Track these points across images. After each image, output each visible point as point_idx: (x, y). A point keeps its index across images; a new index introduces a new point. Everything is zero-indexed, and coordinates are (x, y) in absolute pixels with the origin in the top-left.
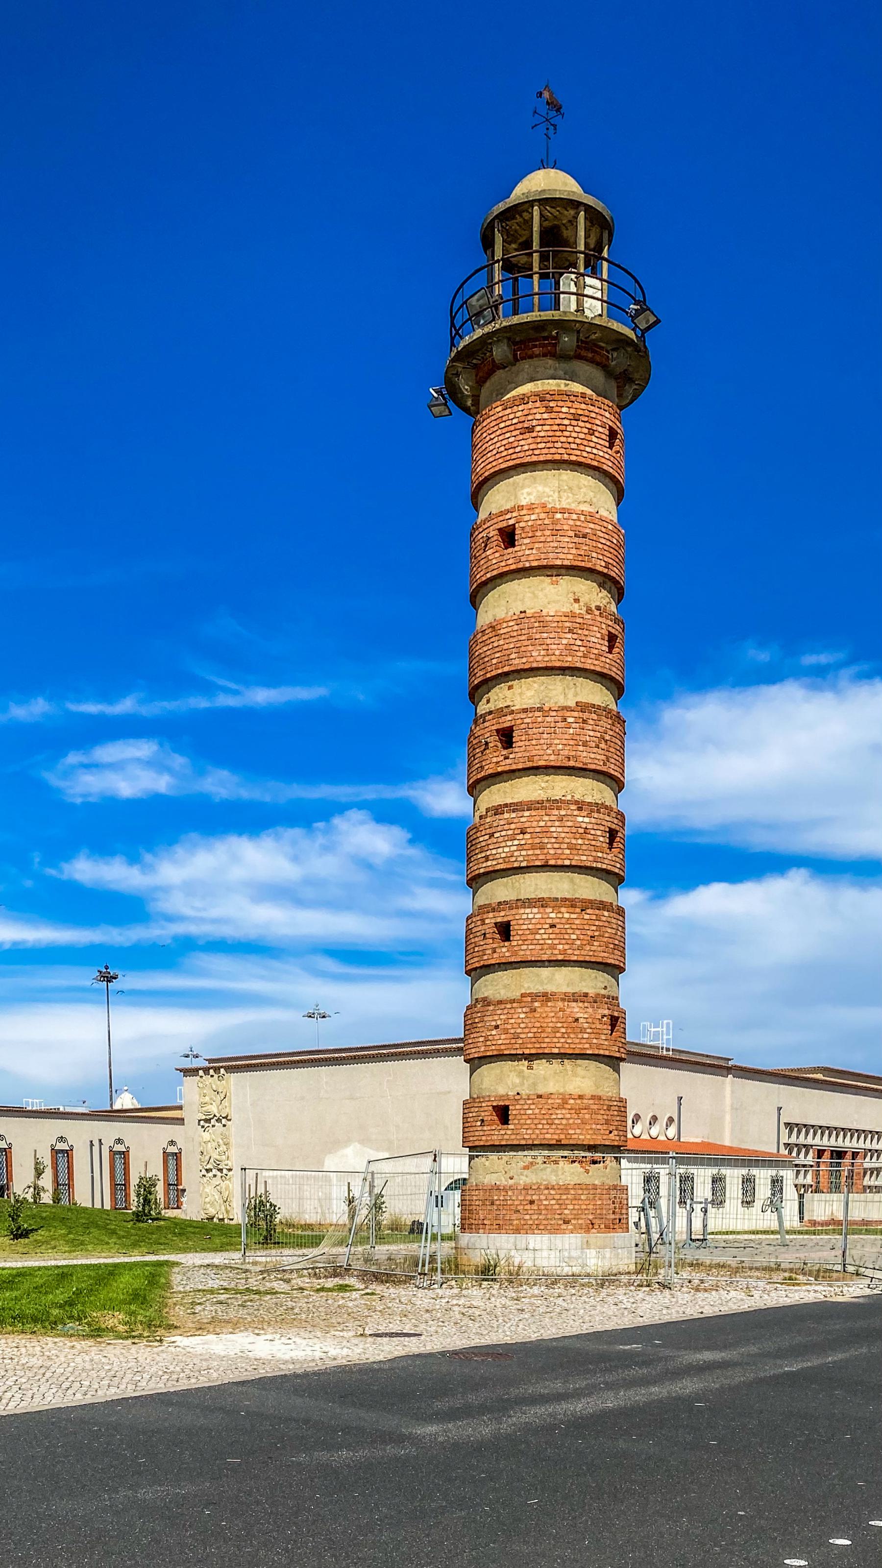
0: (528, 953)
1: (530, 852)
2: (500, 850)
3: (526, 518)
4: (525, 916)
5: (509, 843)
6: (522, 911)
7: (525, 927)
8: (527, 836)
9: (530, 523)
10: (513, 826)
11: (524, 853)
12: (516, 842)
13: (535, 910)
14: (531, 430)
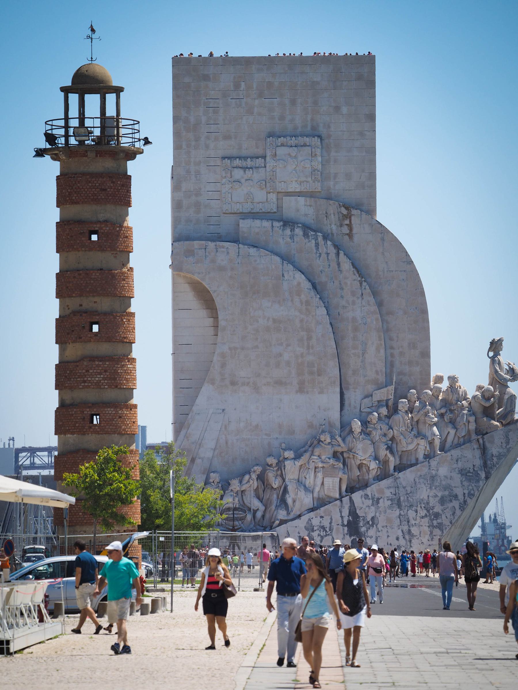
0: (109, 430)
1: (109, 381)
2: (93, 379)
3: (104, 228)
4: (107, 412)
5: (99, 376)
6: (106, 409)
7: (108, 417)
8: (108, 374)
9: (106, 231)
10: (100, 368)
11: (106, 381)
12: (102, 376)
13: (112, 409)
14: (105, 190)
